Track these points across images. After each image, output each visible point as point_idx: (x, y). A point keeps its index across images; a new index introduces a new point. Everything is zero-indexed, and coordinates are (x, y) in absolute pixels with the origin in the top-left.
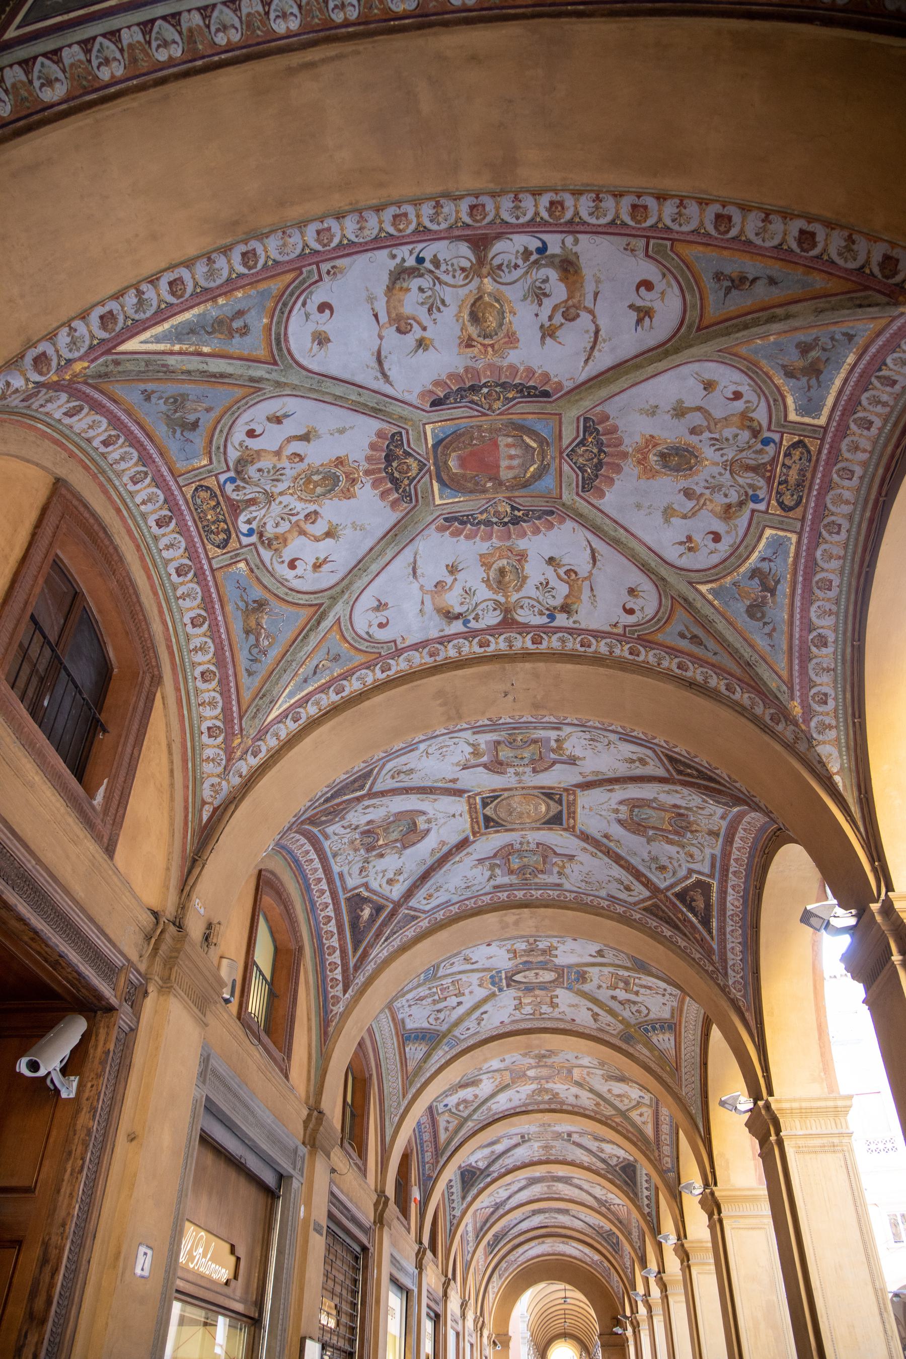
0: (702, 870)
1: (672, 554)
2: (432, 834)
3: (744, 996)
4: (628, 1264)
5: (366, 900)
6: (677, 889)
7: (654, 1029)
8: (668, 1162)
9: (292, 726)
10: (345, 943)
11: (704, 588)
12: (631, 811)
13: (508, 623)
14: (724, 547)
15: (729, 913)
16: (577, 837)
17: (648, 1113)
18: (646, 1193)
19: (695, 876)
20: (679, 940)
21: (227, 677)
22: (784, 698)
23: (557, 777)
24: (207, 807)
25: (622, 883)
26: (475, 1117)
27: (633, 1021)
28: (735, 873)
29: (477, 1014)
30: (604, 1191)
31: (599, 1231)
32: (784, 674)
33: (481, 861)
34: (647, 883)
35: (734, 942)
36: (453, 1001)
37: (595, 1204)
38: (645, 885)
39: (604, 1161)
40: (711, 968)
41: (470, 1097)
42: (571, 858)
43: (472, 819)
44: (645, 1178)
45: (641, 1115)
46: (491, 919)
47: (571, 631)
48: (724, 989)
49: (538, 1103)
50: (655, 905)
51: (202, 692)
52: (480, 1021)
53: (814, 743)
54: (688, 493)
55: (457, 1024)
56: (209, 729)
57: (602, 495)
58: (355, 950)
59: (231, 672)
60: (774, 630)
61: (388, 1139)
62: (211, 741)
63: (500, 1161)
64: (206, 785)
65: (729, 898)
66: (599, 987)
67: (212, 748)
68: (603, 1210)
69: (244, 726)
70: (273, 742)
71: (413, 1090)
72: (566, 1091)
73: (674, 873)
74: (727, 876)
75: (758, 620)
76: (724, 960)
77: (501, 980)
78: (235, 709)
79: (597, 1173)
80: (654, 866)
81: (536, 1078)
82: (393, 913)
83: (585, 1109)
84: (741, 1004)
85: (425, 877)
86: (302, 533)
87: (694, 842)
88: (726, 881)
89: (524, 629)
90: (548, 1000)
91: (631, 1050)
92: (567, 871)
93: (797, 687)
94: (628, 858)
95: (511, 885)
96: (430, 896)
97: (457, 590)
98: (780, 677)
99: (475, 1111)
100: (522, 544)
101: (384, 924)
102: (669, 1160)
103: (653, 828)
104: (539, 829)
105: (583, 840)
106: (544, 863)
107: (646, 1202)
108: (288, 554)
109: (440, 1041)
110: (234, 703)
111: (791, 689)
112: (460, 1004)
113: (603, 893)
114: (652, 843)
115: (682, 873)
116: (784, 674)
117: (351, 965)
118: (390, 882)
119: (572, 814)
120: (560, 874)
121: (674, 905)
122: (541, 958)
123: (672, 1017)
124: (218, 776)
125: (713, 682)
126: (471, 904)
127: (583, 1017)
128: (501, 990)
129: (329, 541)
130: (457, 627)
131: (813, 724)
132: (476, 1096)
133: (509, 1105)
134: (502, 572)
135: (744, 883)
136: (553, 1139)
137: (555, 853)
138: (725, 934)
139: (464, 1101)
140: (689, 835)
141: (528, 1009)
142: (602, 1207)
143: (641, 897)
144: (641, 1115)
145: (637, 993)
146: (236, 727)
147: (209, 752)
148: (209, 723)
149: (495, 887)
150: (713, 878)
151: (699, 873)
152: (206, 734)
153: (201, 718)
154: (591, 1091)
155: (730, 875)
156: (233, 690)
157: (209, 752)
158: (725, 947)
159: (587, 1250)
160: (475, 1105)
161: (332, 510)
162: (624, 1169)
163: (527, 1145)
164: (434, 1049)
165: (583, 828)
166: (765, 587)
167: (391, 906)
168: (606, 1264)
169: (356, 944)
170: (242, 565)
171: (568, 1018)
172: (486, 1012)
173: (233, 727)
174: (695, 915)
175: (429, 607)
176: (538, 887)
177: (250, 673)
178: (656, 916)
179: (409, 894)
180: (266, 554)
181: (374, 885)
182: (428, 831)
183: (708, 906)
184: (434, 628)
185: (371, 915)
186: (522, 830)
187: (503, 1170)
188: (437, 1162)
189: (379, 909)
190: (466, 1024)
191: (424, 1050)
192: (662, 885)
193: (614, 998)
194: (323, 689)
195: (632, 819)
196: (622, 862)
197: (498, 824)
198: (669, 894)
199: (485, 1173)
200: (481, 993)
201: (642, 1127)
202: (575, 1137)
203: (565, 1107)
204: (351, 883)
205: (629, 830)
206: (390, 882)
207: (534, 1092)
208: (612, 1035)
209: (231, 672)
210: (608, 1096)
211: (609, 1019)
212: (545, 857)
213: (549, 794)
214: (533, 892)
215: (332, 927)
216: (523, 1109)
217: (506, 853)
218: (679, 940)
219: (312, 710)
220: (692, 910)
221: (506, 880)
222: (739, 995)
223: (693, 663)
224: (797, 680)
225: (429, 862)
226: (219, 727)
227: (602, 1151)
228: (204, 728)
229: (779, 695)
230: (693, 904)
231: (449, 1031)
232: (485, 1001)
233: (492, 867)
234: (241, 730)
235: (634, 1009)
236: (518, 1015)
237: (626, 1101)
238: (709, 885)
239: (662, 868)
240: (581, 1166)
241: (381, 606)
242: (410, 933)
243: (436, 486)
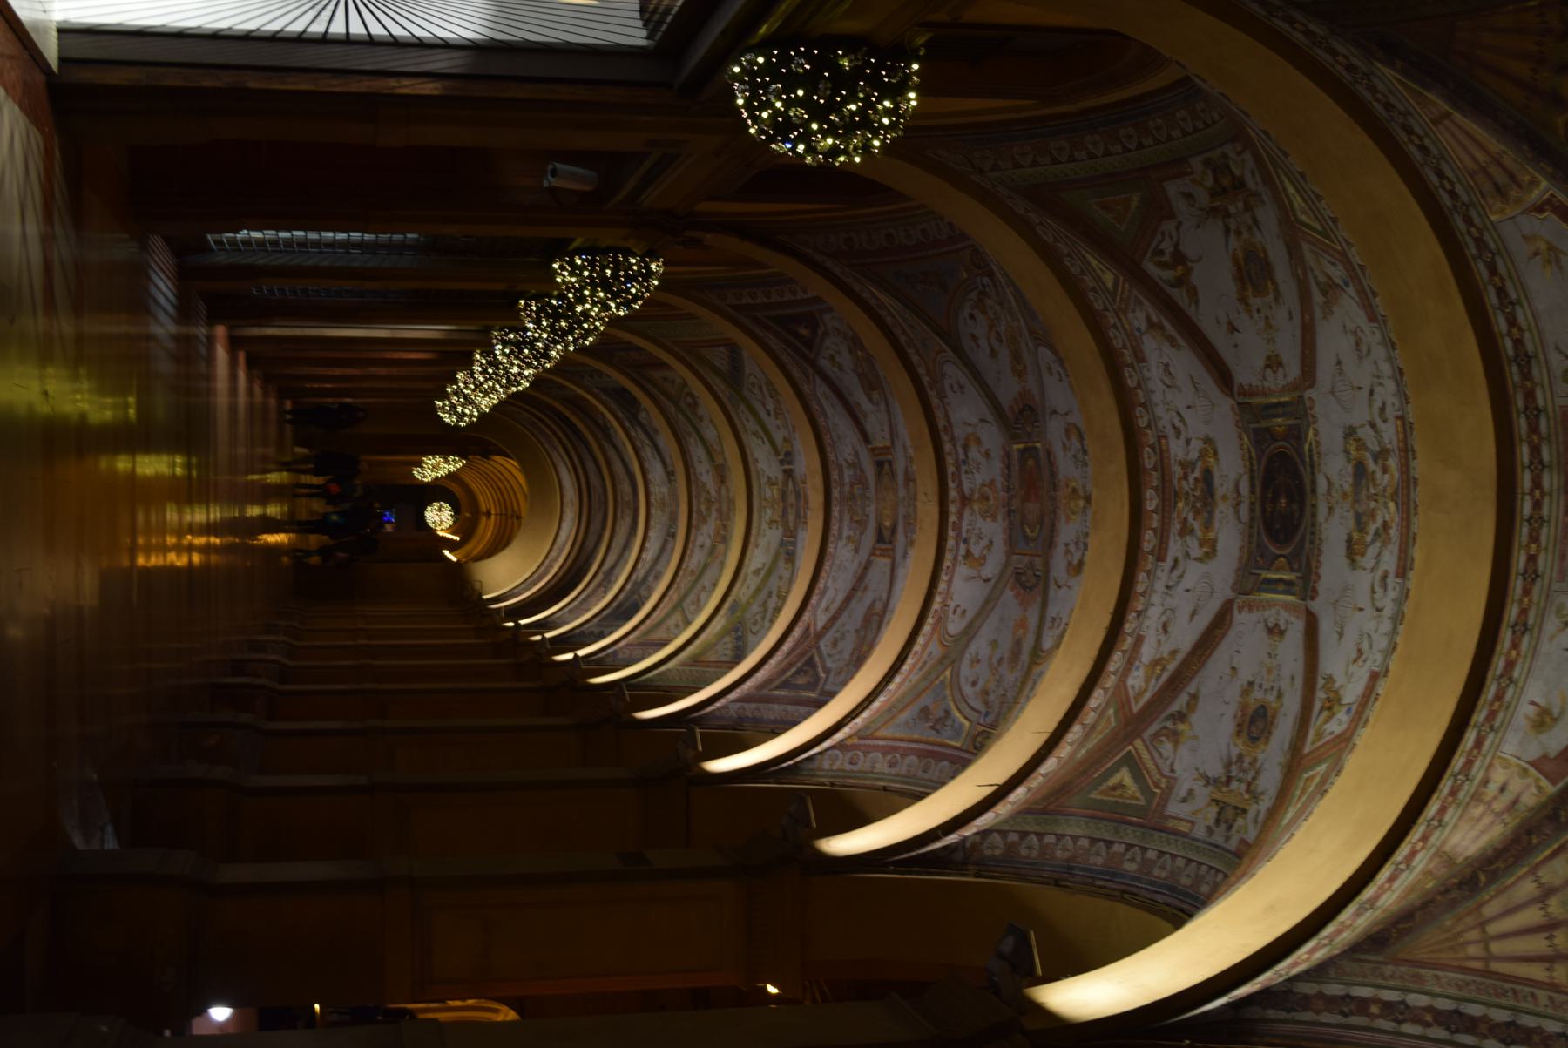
1: (972, 648)
6: (817, 659)
9: (873, 302)
11: (948, 673)
13: (965, 501)
14: (967, 690)
19: (823, 675)
23: (973, 540)
29: (761, 432)
32: (879, 734)
33: (857, 454)
34: (826, 628)
36: (770, 407)
47: (955, 558)
52: (758, 437)
54: (1001, 659)
57: (1013, 589)
70: (857, 287)
86: (991, 327)
89: (960, 515)
97: (979, 458)
100: (1000, 517)
108: (976, 312)
112: (769, 413)
115: (829, 664)
118: (832, 358)
119: (884, 553)
128: (781, 462)
129: (988, 351)
130: (962, 457)
132: (701, 419)
133: (695, 459)
134: (987, 499)
139: (695, 404)
141: (768, 494)
161: (1004, 353)
166: (937, 721)
170: (965, 275)
175: (970, 430)
180: (974, 295)
181: (828, 342)
182: (871, 400)
183: (798, 687)
184: (959, 432)
192: (822, 644)
193: (770, 593)
194: (904, 332)
200: (779, 437)
204: (827, 317)
206: (832, 358)
210: (699, 586)
213: (893, 530)
215: (788, 297)
217: (860, 480)
219: (889, 320)
220: (797, 673)
221: (847, 480)
232: (772, 443)
233: (851, 465)
235: (758, 617)
238: (813, 690)
239: (835, 644)
241: (961, 387)
243: (1021, 446)
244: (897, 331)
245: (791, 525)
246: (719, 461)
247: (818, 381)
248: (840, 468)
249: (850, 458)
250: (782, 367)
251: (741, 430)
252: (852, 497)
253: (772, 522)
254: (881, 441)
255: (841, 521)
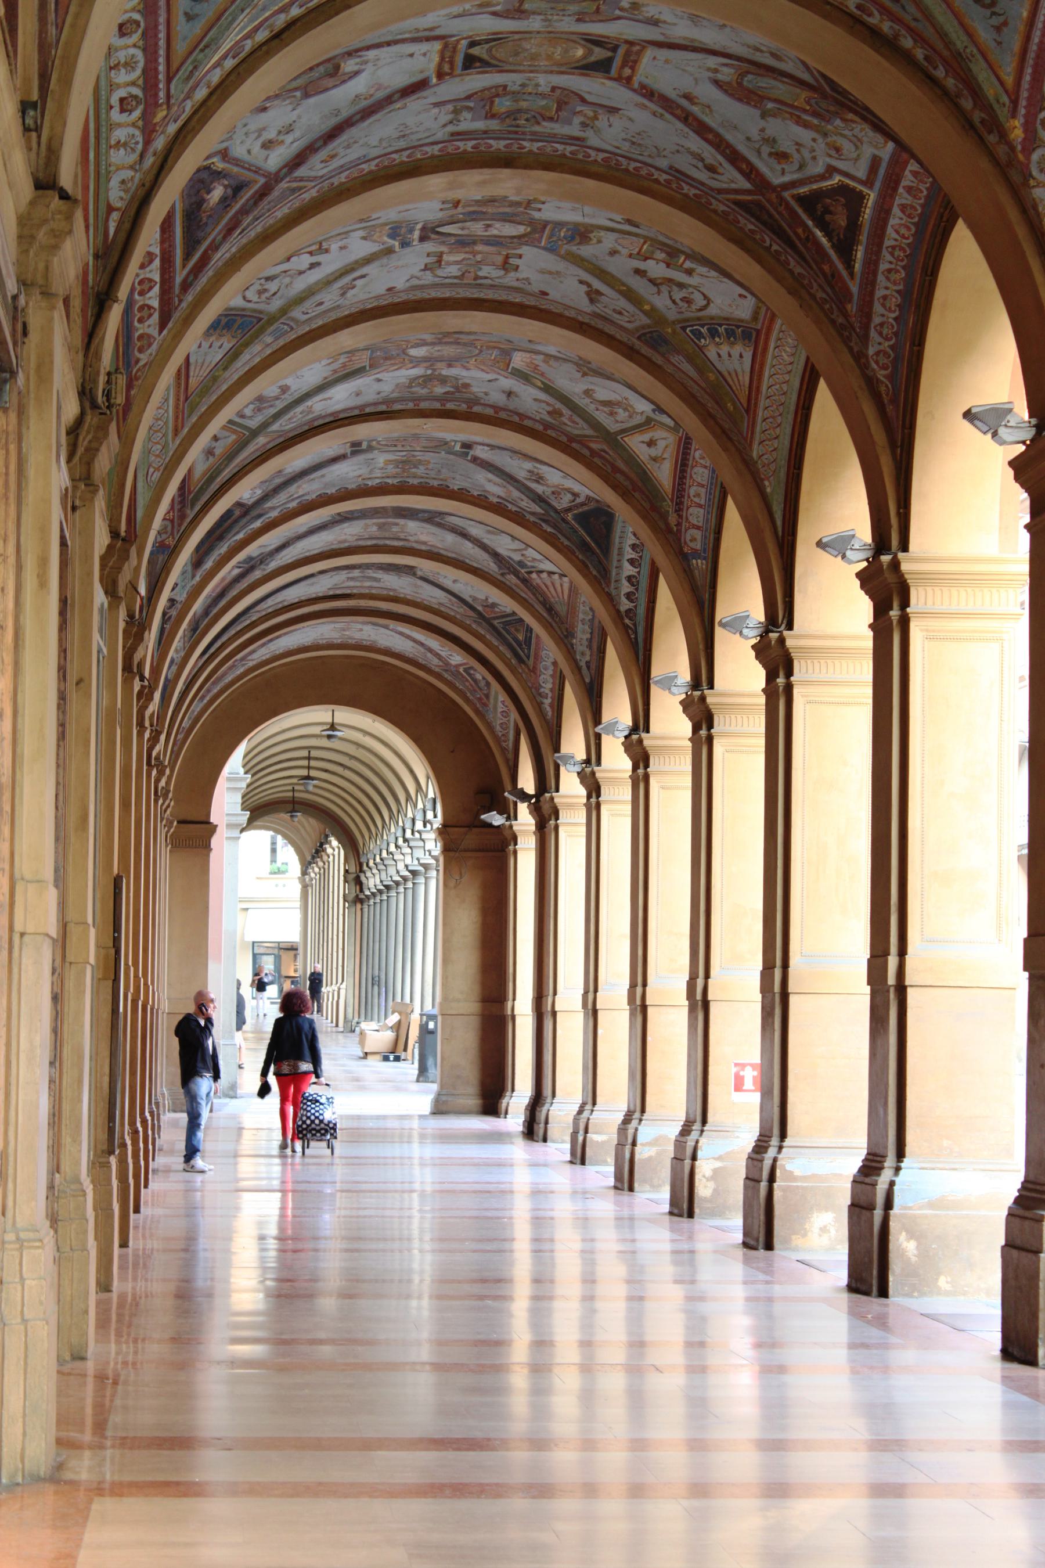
0: (852, 171)
2: (363, 75)
3: (891, 378)
4: (547, 686)
5: (218, 175)
6: (803, 190)
7: (713, 333)
8: (694, 539)
9: (229, 63)
10: (172, 246)
12: (742, 75)
15: (888, 243)
16: (634, 91)
17: (666, 442)
18: (629, 570)
20: (792, 263)
21: (156, 26)
22: (1002, 113)
24: (115, 216)
25: (702, 160)
26: (275, 427)
27: (672, 315)
28: (909, 189)
30: (516, 545)
31: (485, 616)
32: (1009, 80)
33: (436, 105)
35: (887, 288)
36: (306, 260)
37: (492, 567)
38: (747, 176)
39: (539, 499)
40: (841, 320)
41: (272, 391)
42: (613, 110)
43: (442, 58)
44: (631, 540)
45: (651, 443)
46: (436, 182)
48: (860, 358)
49: (417, 400)
50: (758, 204)
51: (116, 50)
53: (1032, 183)
55: (300, 300)
56: (122, 100)
58: (187, 256)
59: (162, 20)
60: (1005, 23)
61: (140, 514)
62: (124, 118)
63: (292, 489)
64: (114, 183)
65: (893, 222)
66: (613, 253)
67: (125, 127)
68: (511, 579)
69: (172, 91)
70: (201, 94)
71: (194, 419)
72: (484, 382)
73: (802, 167)
74: (895, 189)
75: (984, 6)
76: (866, 312)
77: (411, 231)
78: (161, 68)
79: (518, 518)
80: (766, 150)
81: (425, 359)
82: (263, 193)
83: (523, 416)
84: (883, 389)
85: (332, 135)
87: (846, 132)
88: (893, 197)
90: (499, 259)
91: (658, 360)
92: (602, 122)
93: (1023, 103)
94: (721, 131)
95: (485, 132)
96: (332, 157)
98: (1002, 83)
99: (277, 416)
101: (244, 211)
102: (698, 534)
103: (776, 101)
104: (562, 73)
105: (644, 96)
106: (559, 109)
107: (626, 587)
109: (262, 331)
110: (161, 60)
111: (1015, 103)
112: (313, 266)
113: (663, 163)
114: (770, 119)
115: (819, 169)
116: (1009, 80)
117: (178, 280)
118: (268, 145)
119: (631, 61)
120: (584, 125)
121: (793, 213)
122: (508, 210)
123: (755, 317)
124: (132, 167)
125: (907, 43)
126: (404, 157)
127: (569, 290)
128: (405, 244)
131: (1035, 157)
132: (284, 389)
135: (923, 206)
136: (426, 450)
137: (583, 100)
138: (875, 273)
140: (838, 122)
141: (454, 270)
142: (508, 574)
143: (733, 186)
144: (651, 443)
145: (689, 272)
146: (162, 94)
147: (120, 134)
148: (122, 93)
149: (452, 134)
150: (871, 188)
151: (847, 175)
152: (117, 108)
153: (112, 87)
154: (547, 389)
155: (901, 190)
156: (162, 43)
157: (120, 134)
158: (872, 294)
159: (434, 642)
160: (280, 405)
162: (584, 519)
163: (361, 458)
164: (247, 345)
165: (646, 81)
167: (262, 181)
168: (481, 673)
169: (191, 244)
171: (535, 288)
172: (363, 276)
173: (156, 95)
174: (828, 234)
176: (536, 137)
177: (189, 17)
178: (758, 219)
179: (299, 160)
181: (239, 151)
185: (224, 199)
186: (531, 72)
187: (293, 505)
188: (182, 517)
189: (238, 189)
190: (318, 298)
191: (227, 346)
192: (777, 180)
193: (638, 272)
195: (740, 84)
196: (710, 136)
197: (485, 63)
198: (786, 194)
199: (254, 513)
200: (359, 248)
201: (650, 466)
202: (480, 452)
203: (477, 409)
205: (731, 95)
206: (268, 145)
207: (413, 380)
208: (621, 328)
209: (162, 20)
210: (583, 402)
211: (622, 303)
212: (561, 105)
214: (525, 143)
216: (383, 408)
218: (792, 263)
219: (262, 36)
221: (480, 125)
222: (881, 374)
223: (881, 14)
224: (1024, 94)
225: (345, 114)
226: (136, 97)
227: (539, 479)
228: (115, 100)
229: (996, 106)
230: (828, 217)
231: (284, 311)
233: (456, 112)
234: (168, 96)
235: (678, 295)
236: (428, 278)
237: (622, 415)
238: (861, 197)
239: (782, 156)
240: (481, 502)
242: (282, 212)
244: (281, 20)
245: (521, 229)
246: (363, 359)
247: (302, 172)
248: (457, 135)
249: (445, 118)
250: (267, 238)
251: (333, 316)
252: (513, 114)
253: (506, 265)
254: (424, 59)
255: (553, 138)
